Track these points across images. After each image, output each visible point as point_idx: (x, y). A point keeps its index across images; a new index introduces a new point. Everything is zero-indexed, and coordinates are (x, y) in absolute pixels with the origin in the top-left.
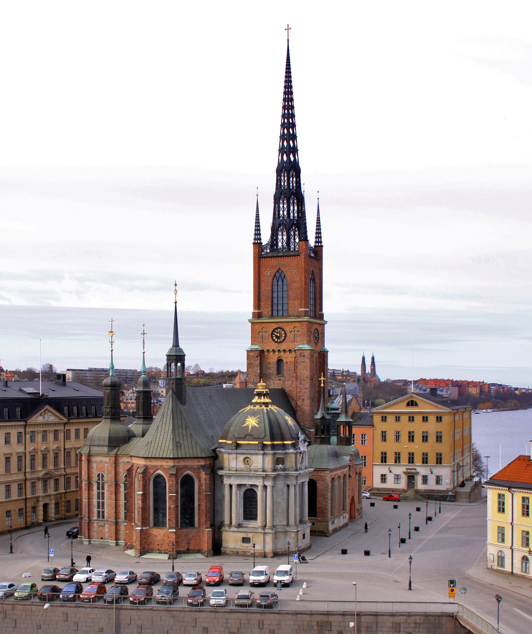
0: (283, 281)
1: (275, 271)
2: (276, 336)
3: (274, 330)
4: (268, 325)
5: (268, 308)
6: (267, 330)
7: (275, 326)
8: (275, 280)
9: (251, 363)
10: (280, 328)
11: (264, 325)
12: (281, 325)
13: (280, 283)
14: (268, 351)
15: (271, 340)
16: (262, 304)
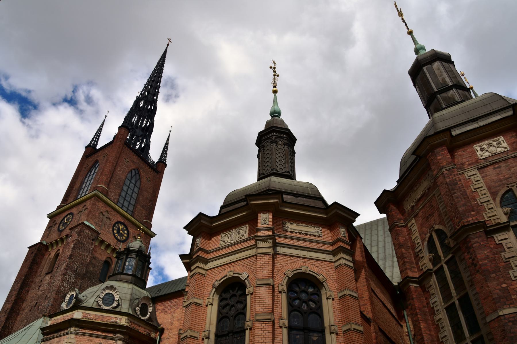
0: (136, 182)
1: (133, 166)
2: (119, 230)
3: (118, 222)
4: (114, 213)
5: (116, 195)
6: (111, 217)
7: (120, 219)
8: (129, 175)
9: (82, 243)
10: (125, 226)
11: (109, 209)
12: (127, 223)
13: (133, 181)
14: (102, 242)
15: (111, 232)
16: (112, 187)
